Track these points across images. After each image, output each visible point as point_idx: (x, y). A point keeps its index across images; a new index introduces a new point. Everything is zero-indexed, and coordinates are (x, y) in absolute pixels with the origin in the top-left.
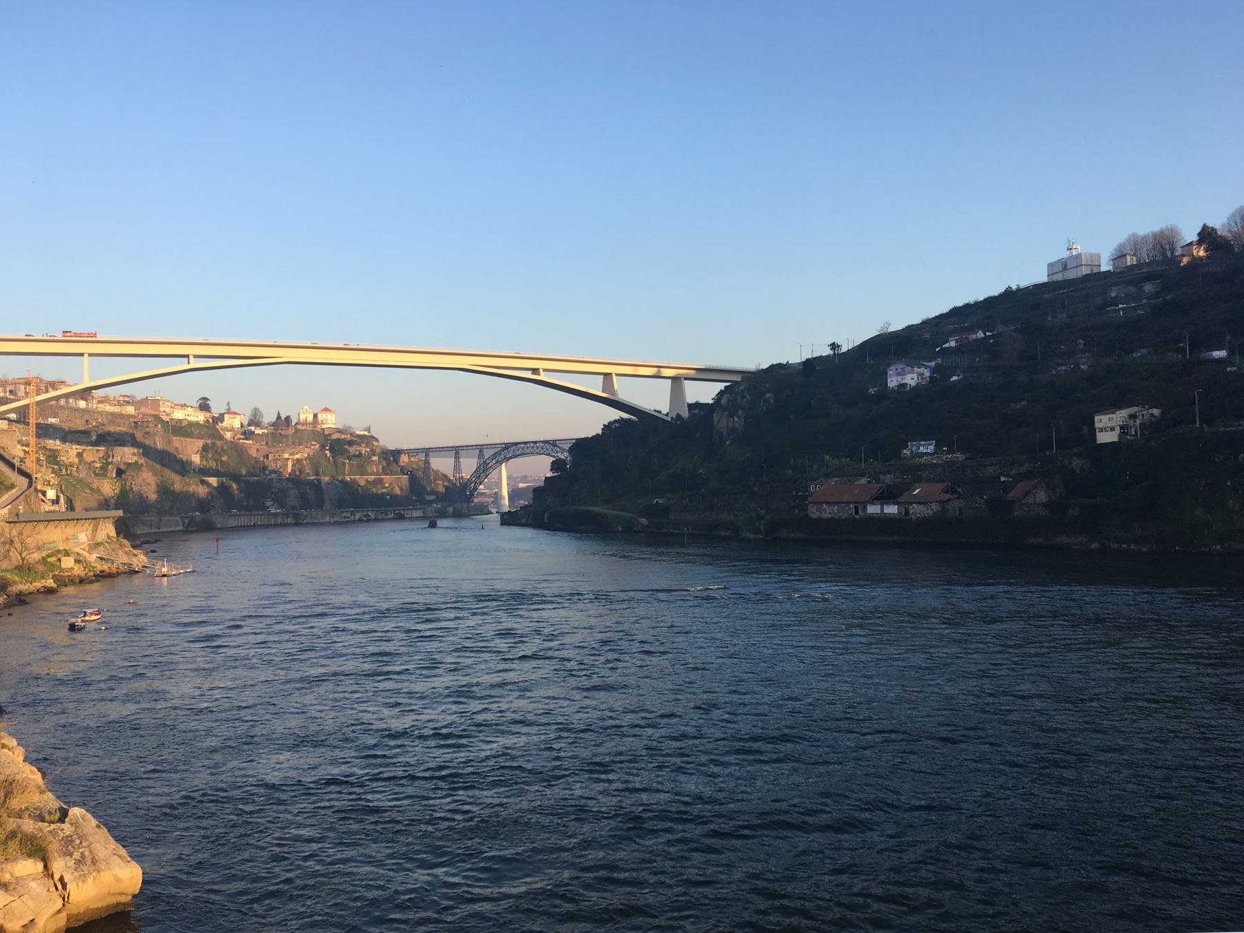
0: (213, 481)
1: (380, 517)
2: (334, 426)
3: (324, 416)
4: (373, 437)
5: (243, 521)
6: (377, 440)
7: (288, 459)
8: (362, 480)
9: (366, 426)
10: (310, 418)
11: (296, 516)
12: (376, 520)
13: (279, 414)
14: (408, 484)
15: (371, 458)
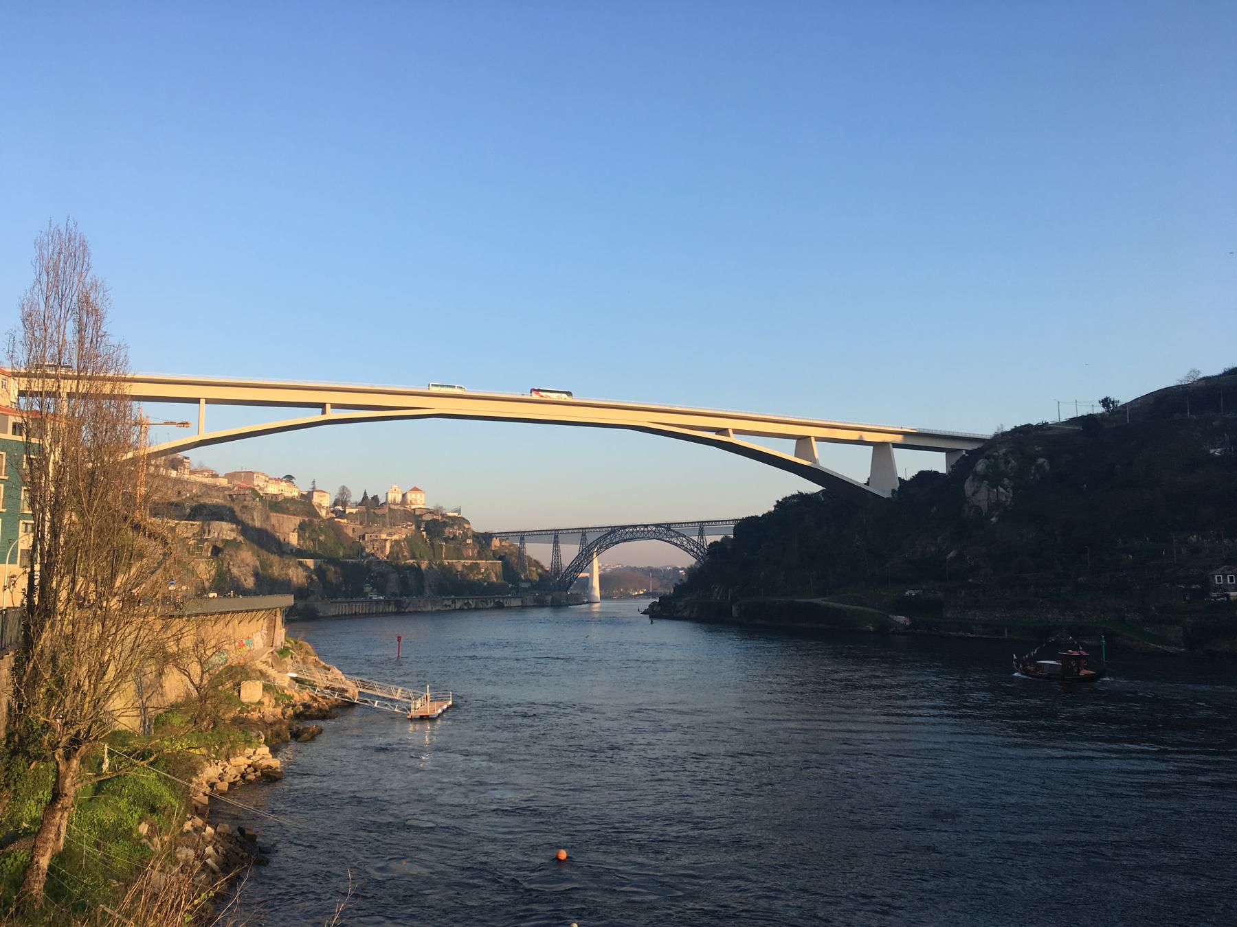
0: (310, 562)
1: (481, 606)
2: (422, 507)
3: (413, 495)
4: (464, 519)
5: (345, 609)
6: (469, 523)
7: (386, 540)
8: (459, 565)
9: (456, 507)
10: (399, 498)
11: (398, 604)
12: (476, 609)
13: (365, 493)
14: (501, 571)
15: (465, 541)
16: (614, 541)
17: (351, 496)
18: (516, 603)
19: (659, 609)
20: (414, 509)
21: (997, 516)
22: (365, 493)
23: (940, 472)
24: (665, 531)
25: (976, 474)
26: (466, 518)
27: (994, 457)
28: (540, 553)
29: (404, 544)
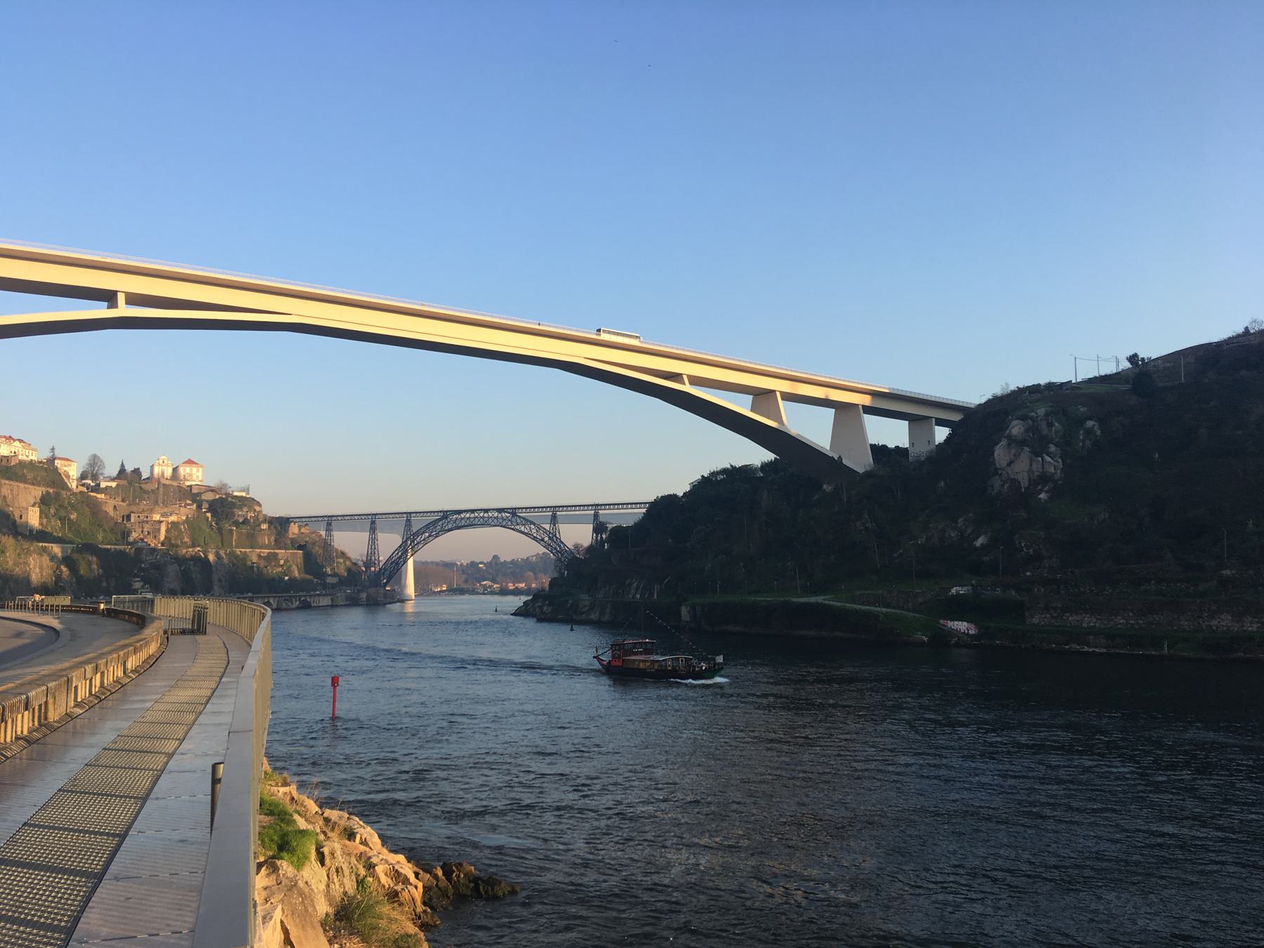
0: (56, 549)
1: (284, 606)
2: (199, 483)
3: (188, 470)
7: (160, 522)
8: (253, 555)
9: (244, 485)
13: (123, 465)
14: (302, 563)
15: (259, 525)
16: (446, 528)
17: (104, 467)
18: (326, 601)
19: (550, 610)
20: (191, 486)
21: (1046, 492)
22: (122, 463)
23: (889, 446)
24: (511, 517)
25: (1009, 437)
26: (256, 499)
27: (1031, 418)
28: (351, 544)
29: (184, 527)
